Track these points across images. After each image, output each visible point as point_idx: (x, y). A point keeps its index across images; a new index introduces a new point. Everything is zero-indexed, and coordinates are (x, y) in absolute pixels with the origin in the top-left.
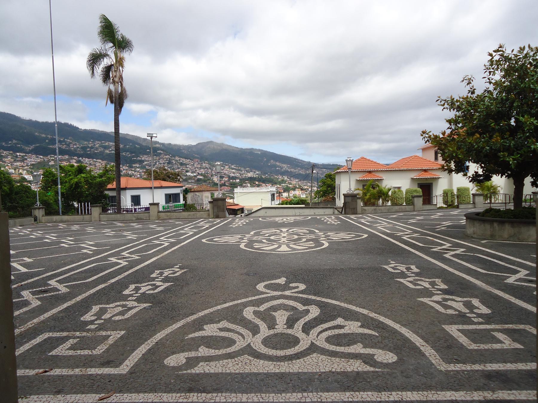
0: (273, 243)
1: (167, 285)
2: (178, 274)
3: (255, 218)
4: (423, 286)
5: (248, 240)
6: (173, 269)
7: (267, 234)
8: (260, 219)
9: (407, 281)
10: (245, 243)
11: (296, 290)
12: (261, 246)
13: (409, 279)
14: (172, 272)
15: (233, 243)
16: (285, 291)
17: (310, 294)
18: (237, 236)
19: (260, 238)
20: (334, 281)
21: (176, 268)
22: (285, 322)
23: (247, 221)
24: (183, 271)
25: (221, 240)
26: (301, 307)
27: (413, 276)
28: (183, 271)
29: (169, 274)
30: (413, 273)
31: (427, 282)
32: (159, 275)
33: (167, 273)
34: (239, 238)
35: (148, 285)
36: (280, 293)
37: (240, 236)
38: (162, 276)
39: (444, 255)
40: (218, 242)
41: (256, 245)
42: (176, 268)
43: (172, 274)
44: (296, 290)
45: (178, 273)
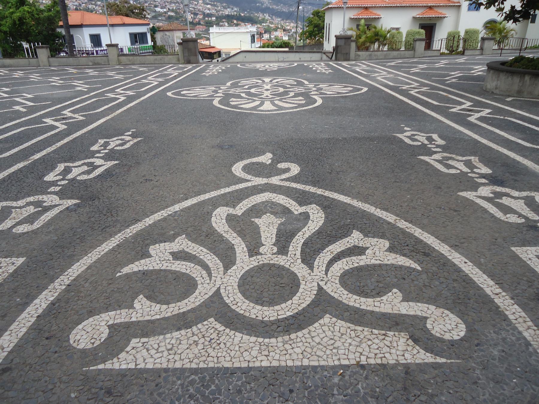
1: (110, 164)
2: (127, 146)
3: (233, 64)
5: (223, 94)
6: (123, 137)
8: (239, 65)
10: (220, 98)
12: (240, 103)
14: (120, 142)
15: (205, 97)
18: (211, 88)
19: (238, 90)
21: (127, 135)
23: (224, 68)
25: (190, 94)
29: (116, 146)
32: (102, 148)
33: (114, 143)
34: (212, 91)
37: (214, 88)
40: (186, 96)
41: (234, 102)
42: (127, 135)
45: (128, 144)
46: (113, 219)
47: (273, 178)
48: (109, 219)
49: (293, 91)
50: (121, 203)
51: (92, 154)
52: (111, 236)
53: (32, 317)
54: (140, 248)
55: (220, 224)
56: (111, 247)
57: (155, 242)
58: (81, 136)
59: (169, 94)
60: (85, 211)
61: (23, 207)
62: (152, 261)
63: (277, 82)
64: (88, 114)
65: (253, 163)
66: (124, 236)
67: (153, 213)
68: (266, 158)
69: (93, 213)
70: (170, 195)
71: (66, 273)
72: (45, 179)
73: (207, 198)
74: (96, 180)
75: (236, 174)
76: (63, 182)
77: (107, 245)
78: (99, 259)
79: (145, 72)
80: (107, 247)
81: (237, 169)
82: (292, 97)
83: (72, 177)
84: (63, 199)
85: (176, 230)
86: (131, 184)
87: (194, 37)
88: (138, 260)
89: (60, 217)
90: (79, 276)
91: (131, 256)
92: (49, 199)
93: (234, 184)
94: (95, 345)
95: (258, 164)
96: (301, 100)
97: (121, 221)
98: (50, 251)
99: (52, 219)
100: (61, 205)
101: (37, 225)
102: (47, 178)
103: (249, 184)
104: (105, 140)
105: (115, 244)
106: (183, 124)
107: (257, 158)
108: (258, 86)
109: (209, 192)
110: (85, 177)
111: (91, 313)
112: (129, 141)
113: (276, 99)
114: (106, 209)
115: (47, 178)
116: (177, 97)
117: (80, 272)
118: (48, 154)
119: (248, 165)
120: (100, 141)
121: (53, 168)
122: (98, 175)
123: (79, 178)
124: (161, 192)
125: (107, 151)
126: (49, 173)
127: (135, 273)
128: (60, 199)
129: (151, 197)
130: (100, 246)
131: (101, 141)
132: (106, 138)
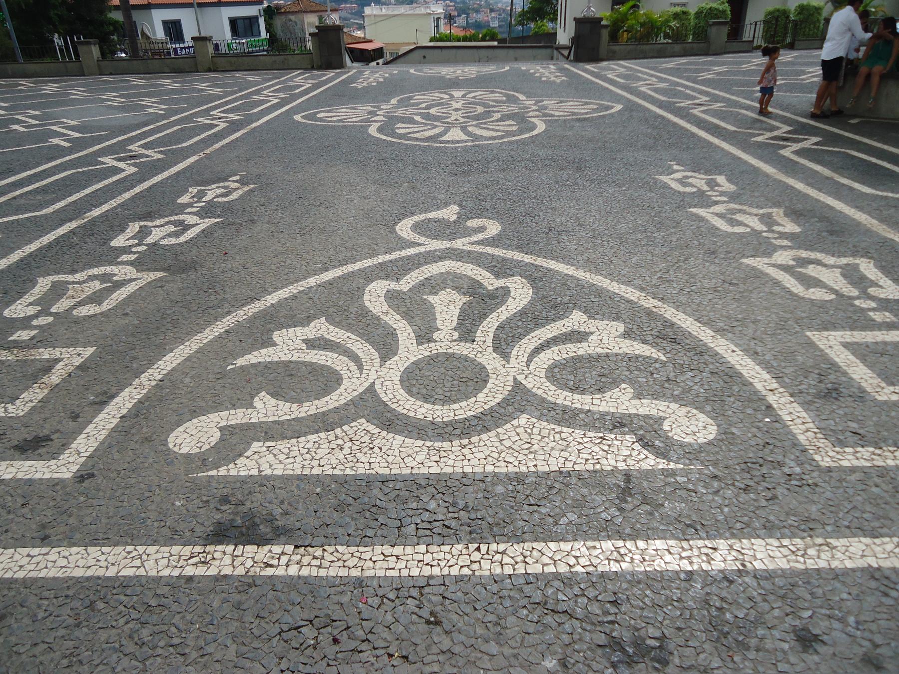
0: (435, 123)
1: (208, 222)
2: (234, 196)
4: (747, 226)
5: (384, 116)
6: (226, 184)
7: (424, 102)
9: (712, 213)
10: (379, 124)
11: (480, 237)
12: (411, 130)
13: (718, 209)
14: (223, 190)
15: (356, 122)
16: (456, 238)
17: (509, 247)
18: (364, 108)
19: (409, 111)
20: (560, 215)
21: (234, 181)
22: (455, 324)
24: (246, 189)
25: (331, 117)
26: (491, 282)
27: (725, 202)
28: (246, 189)
29: (217, 197)
30: (722, 194)
31: (756, 215)
33: (212, 193)
35: (169, 223)
36: (446, 244)
37: (370, 108)
38: (200, 202)
41: (402, 128)
42: (234, 181)
43: (222, 195)
44: (480, 237)
45: (234, 194)
46: (218, 296)
47: (458, 241)
48: (213, 297)
49: (499, 111)
50: (230, 276)
51: (182, 208)
52: (216, 319)
53: (113, 417)
54: (259, 335)
55: (376, 304)
56: (217, 334)
57: (281, 326)
58: (162, 182)
59: (297, 118)
60: (176, 286)
61: (84, 282)
62: (277, 351)
63: (474, 97)
64: (169, 150)
65: (429, 220)
66: (236, 319)
67: (277, 289)
68: (450, 213)
69: (189, 290)
70: (302, 265)
71: (156, 366)
72: (112, 244)
73: (357, 268)
74: (190, 245)
75: (402, 235)
76: (140, 249)
77: (211, 331)
78: (200, 348)
79: (256, 83)
80: (211, 333)
81: (405, 228)
82: (497, 121)
83: (152, 241)
84: (143, 271)
85: (312, 312)
86: (242, 250)
87: (338, 23)
88: (258, 349)
89: (140, 295)
90: (173, 370)
91: (247, 345)
92: (120, 272)
93: (399, 250)
94: (203, 450)
95: (436, 220)
96: (511, 125)
97: (230, 299)
98: (130, 339)
99: (129, 297)
100: (140, 279)
101: (106, 306)
102: (114, 243)
103: (422, 249)
104: (199, 188)
105: (223, 330)
106: (320, 163)
107: (435, 213)
108: (442, 104)
109: (361, 261)
110: (173, 241)
111: (195, 413)
112: (236, 189)
113: (471, 123)
114: (207, 284)
115: (114, 243)
116: (310, 122)
117: (174, 365)
118: (113, 209)
119: (421, 223)
120: (190, 189)
121: (122, 229)
122: (193, 238)
123: (162, 242)
124: (289, 262)
125: (203, 204)
126: (116, 236)
127: (253, 366)
128: (138, 271)
129: (273, 267)
130: (201, 333)
131: (194, 190)
132: (200, 185)
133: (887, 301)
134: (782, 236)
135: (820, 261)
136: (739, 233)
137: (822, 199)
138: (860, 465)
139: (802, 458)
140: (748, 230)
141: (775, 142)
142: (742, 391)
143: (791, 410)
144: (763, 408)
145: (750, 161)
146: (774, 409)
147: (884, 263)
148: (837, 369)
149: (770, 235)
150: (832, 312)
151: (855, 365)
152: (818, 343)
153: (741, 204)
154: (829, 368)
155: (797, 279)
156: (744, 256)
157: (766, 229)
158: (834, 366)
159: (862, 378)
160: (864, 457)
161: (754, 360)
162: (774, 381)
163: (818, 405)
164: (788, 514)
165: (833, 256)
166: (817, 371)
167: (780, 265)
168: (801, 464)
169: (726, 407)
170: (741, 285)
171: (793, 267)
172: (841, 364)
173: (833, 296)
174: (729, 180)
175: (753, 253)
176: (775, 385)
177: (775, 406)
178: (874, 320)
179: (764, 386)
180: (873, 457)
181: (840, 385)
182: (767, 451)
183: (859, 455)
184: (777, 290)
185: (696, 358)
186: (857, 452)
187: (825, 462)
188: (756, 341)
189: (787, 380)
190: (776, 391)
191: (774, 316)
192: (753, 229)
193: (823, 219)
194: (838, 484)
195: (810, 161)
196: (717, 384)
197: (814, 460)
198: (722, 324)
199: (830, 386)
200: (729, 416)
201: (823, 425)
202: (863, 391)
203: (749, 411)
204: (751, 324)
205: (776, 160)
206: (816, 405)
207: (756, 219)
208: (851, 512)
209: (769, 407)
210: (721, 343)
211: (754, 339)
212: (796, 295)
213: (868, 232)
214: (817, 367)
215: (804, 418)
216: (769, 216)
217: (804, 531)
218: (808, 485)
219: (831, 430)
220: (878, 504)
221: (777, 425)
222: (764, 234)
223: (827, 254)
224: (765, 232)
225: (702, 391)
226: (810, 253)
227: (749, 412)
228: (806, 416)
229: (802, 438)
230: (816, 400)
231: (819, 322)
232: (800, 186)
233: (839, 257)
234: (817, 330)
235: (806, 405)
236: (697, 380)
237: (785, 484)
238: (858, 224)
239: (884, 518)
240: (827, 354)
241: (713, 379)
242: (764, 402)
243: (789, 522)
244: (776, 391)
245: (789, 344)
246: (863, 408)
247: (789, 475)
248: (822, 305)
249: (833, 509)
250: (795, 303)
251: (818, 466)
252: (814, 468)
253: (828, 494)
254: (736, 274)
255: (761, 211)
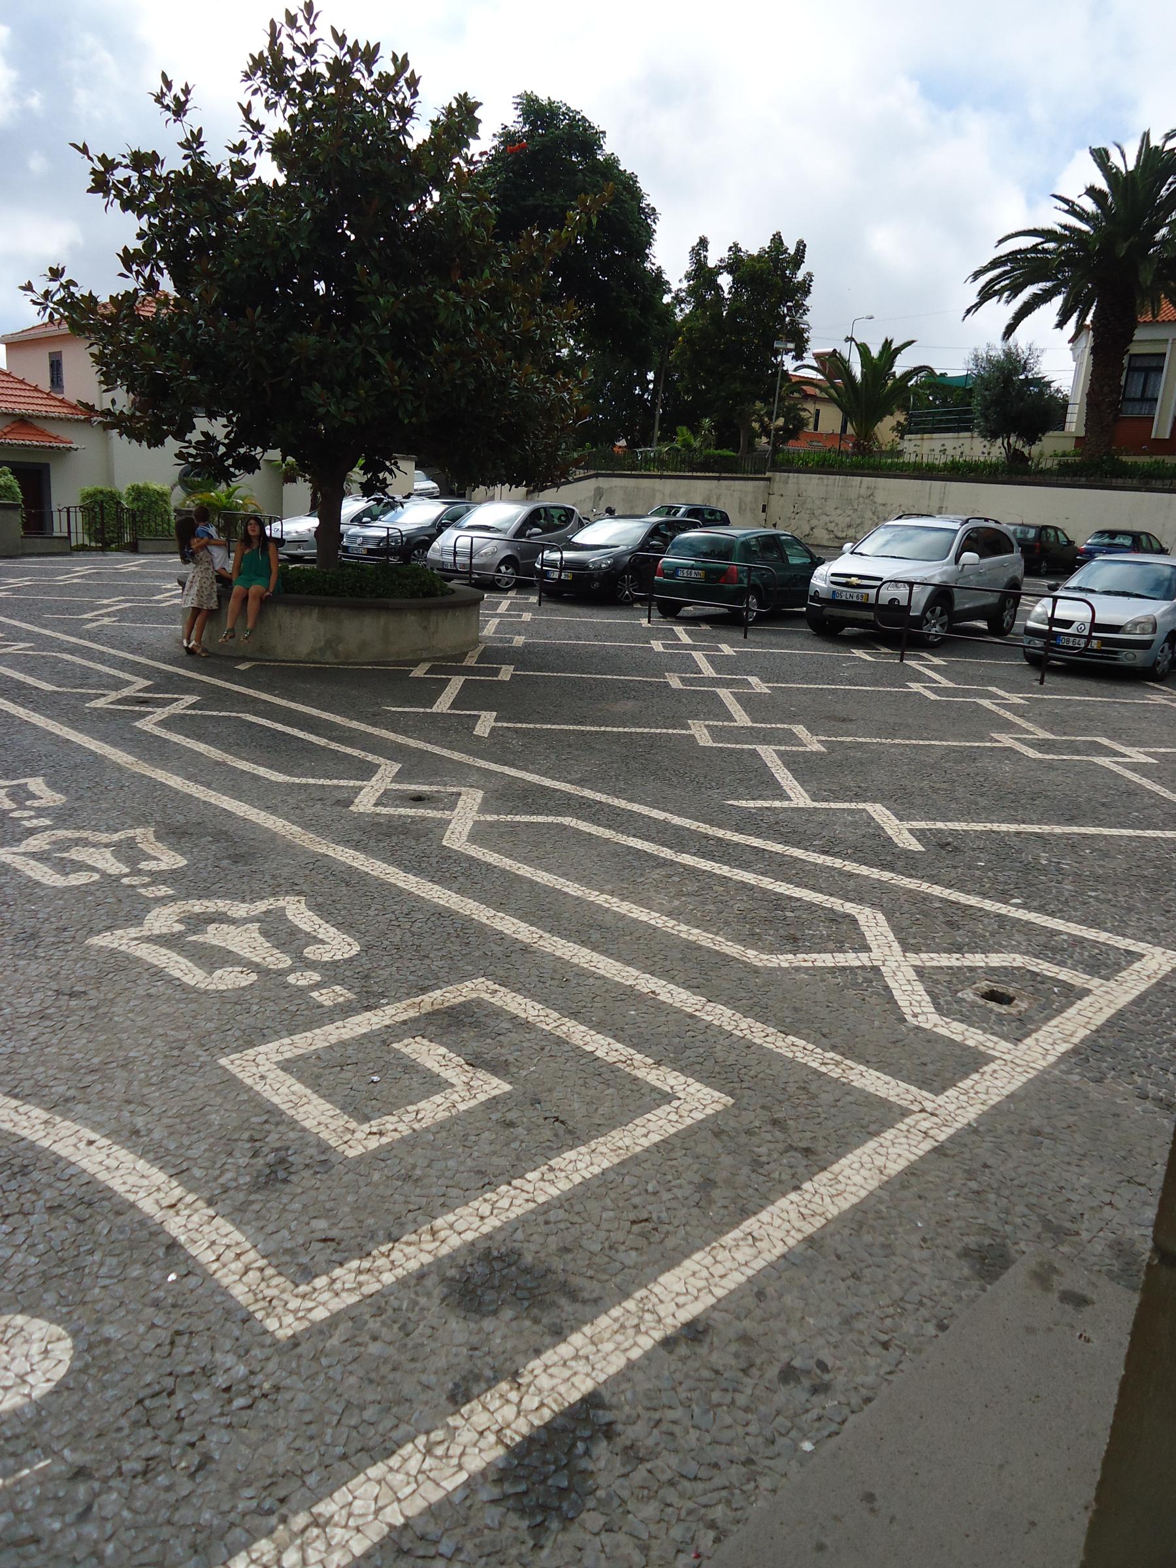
4: (93, 869)
9: (24, 854)
13: (35, 843)
27: (47, 828)
30: (41, 812)
31: (107, 846)
39: (138, 724)
133: (335, 964)
134: (157, 878)
135: (225, 914)
136: (78, 887)
137: (212, 801)
138: (343, 1306)
139: (246, 1338)
140: (96, 877)
141: (126, 708)
142: (115, 1230)
143: (214, 1237)
144: (161, 1252)
145: (86, 745)
146: (181, 1247)
147: (320, 900)
148: (278, 1119)
149: (135, 881)
150: (255, 1008)
151: (305, 1100)
152: (240, 1076)
153: (78, 828)
154: (266, 1122)
155: (190, 957)
156: (92, 932)
157: (127, 870)
158: (273, 1114)
159: (319, 1124)
160: (347, 1286)
161: (132, 1149)
162: (174, 1183)
163: (256, 1207)
164: (234, 1489)
165: (243, 901)
166: (246, 1136)
167: (158, 936)
168: (243, 1353)
169: (87, 1281)
170: (93, 993)
171: (181, 935)
172: (283, 1107)
173: (254, 977)
174: (52, 785)
175: (108, 923)
176: (178, 1192)
177: (182, 1239)
178: (321, 1006)
179: (157, 1202)
180: (362, 1278)
181: (288, 1149)
182: (179, 1350)
183: (338, 1286)
184: (160, 988)
185: (13, 1184)
186: (333, 1281)
187: (283, 1326)
188: (132, 1107)
189: (197, 1172)
190: (180, 1206)
191: (158, 1042)
192: (104, 874)
193: (220, 836)
194: (315, 1367)
195: (187, 736)
196: (63, 1229)
197: (266, 1332)
198: (62, 1089)
199: (271, 1158)
200: (95, 1302)
201: (272, 1246)
202: (324, 1148)
203: (136, 1271)
204: (119, 1072)
205: (131, 740)
206: (256, 1207)
207: (108, 853)
208: (344, 1421)
209: (173, 1246)
210: (64, 1133)
211: (129, 1102)
212: (194, 989)
213: (290, 848)
214: (246, 1125)
215: (238, 1244)
216: (131, 843)
217: (270, 1512)
218: (265, 1396)
219: (286, 1251)
220: (383, 1377)
221: (192, 1281)
222: (125, 881)
223: (233, 899)
224: (126, 875)
225: (33, 1260)
226: (206, 903)
227: (135, 1274)
228: (239, 1237)
229: (239, 1292)
230: (252, 1197)
231: (238, 1033)
232: (175, 782)
233: (252, 901)
234: (237, 1050)
235: (238, 1215)
236: (20, 1237)
237: (222, 1414)
238: (273, 836)
239: (398, 1403)
240: (258, 1093)
241: (55, 1223)
242: (161, 1237)
243: (241, 1506)
244: (180, 1206)
245: (192, 1094)
246: (330, 1183)
247: (228, 1389)
248: (237, 999)
249: (313, 1430)
250: (193, 1006)
251: (276, 1342)
252: (268, 1352)
253: (302, 1399)
254: (80, 972)
255: (116, 837)
